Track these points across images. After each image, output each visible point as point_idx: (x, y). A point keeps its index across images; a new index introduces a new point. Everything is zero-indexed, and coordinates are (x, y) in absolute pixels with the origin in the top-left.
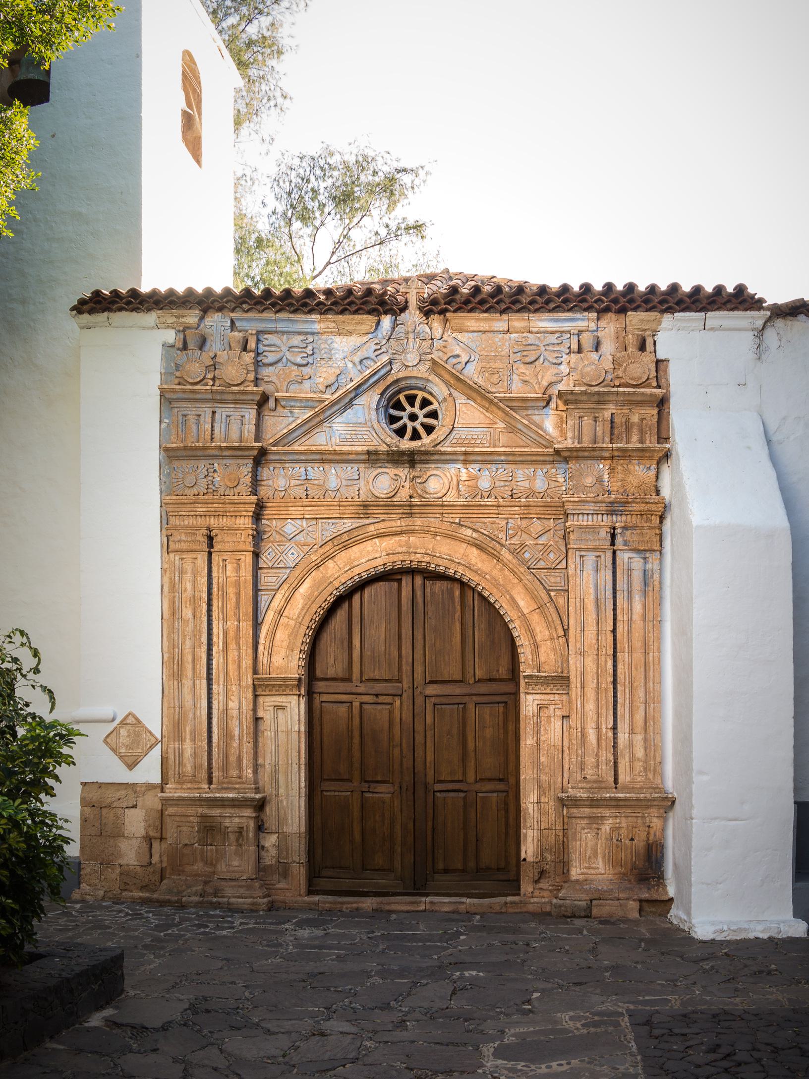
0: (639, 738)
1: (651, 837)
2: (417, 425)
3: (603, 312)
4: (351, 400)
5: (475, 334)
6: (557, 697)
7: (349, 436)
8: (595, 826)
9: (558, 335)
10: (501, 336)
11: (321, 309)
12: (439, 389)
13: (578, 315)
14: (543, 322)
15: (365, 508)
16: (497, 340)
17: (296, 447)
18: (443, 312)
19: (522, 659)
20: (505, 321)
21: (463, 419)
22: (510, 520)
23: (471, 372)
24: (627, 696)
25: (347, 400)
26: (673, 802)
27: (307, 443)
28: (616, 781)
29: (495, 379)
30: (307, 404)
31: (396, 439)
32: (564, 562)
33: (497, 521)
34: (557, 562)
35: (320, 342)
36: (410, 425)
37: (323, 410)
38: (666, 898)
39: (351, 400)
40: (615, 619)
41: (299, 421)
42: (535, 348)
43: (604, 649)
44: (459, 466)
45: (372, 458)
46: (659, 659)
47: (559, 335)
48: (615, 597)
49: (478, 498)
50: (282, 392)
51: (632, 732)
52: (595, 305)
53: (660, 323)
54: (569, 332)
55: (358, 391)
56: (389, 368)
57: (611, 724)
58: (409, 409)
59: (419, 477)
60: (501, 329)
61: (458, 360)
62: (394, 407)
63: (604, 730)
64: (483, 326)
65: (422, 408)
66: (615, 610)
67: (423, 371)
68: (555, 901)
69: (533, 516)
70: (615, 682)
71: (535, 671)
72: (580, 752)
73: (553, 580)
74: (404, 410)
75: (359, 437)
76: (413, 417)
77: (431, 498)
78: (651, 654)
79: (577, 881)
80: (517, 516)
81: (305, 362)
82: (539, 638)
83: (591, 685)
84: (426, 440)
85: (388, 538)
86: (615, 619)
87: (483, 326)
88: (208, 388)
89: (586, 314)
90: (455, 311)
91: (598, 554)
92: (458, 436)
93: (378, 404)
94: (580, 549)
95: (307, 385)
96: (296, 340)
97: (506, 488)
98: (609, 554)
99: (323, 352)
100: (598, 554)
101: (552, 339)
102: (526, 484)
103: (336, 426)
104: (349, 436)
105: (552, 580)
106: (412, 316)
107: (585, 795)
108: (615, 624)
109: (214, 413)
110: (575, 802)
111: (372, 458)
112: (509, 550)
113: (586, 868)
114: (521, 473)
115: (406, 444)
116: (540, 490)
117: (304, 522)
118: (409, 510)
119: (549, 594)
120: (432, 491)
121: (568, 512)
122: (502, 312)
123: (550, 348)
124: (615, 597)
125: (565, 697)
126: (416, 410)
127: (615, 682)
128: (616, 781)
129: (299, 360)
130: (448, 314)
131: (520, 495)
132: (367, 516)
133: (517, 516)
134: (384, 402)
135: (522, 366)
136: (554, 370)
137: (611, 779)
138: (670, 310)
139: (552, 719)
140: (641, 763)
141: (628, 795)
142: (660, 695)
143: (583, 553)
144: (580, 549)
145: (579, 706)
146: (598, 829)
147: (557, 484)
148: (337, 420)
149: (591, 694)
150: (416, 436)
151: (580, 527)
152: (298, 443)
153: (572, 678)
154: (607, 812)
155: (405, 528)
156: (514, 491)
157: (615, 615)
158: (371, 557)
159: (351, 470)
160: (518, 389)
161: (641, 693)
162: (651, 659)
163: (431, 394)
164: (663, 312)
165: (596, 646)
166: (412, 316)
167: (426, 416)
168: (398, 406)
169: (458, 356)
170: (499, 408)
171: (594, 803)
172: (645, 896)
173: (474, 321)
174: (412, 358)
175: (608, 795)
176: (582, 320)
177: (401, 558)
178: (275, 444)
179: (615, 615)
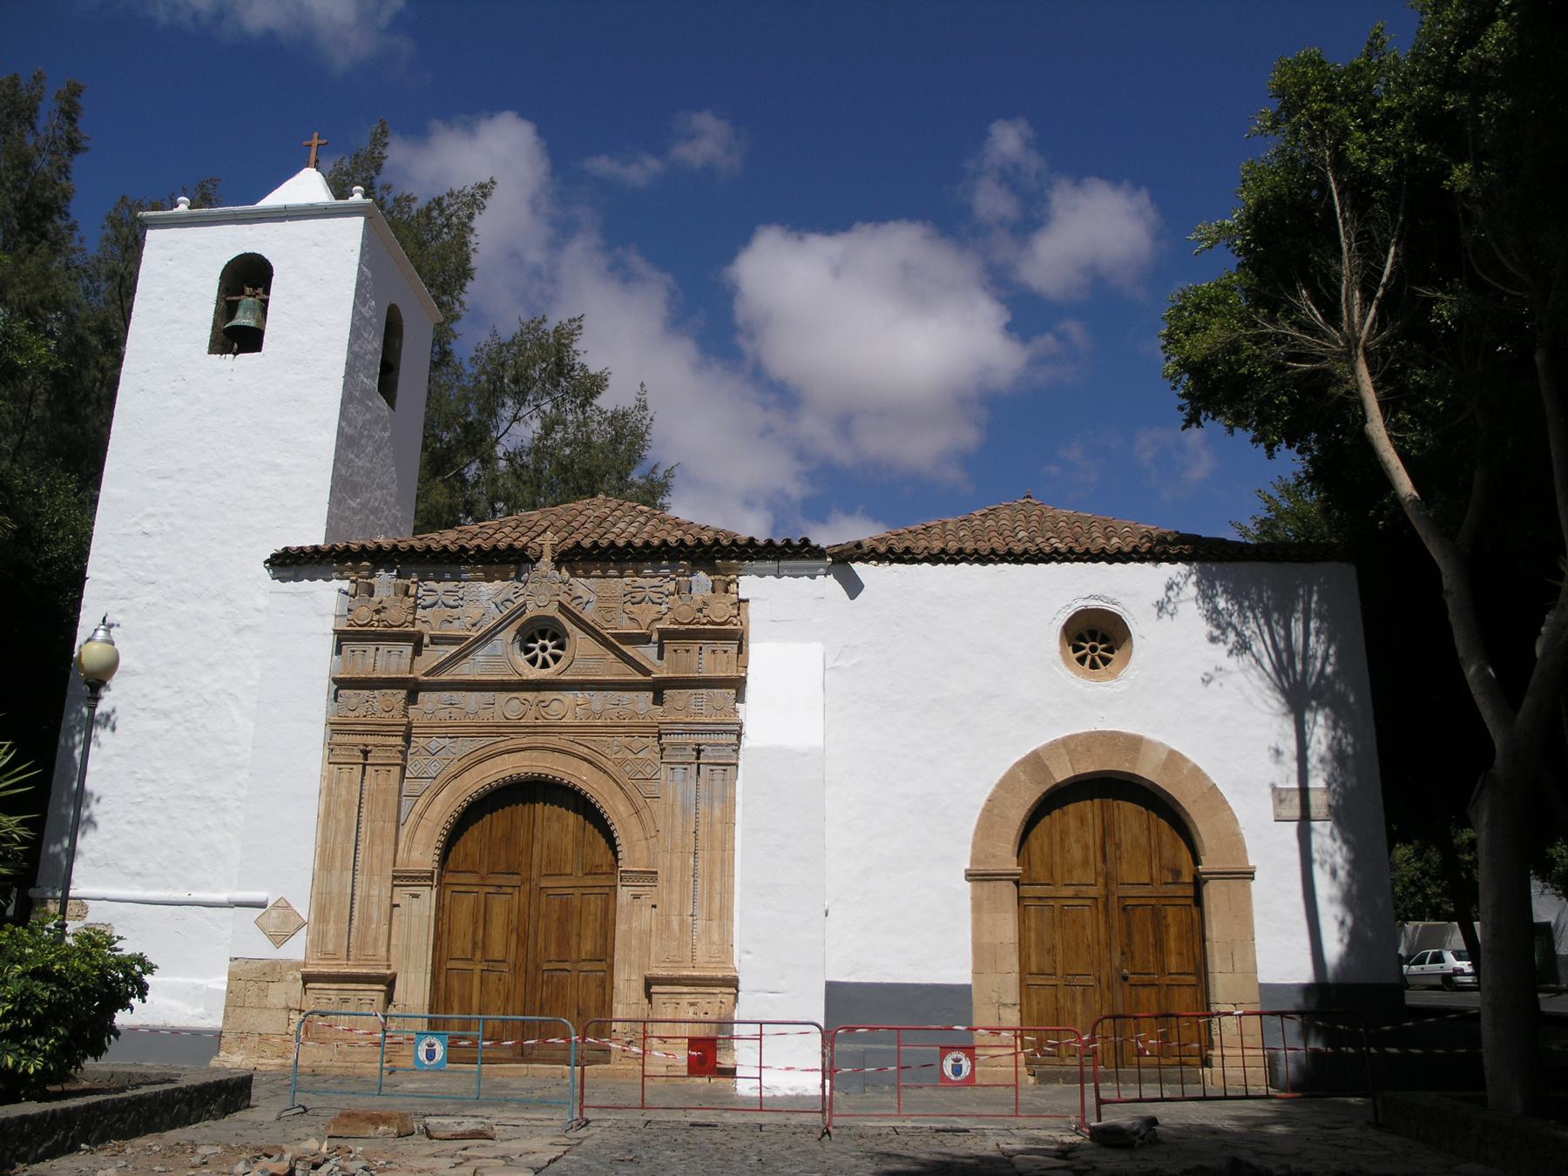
12: (569, 626)
15: (497, 730)
23: (589, 615)
36: (541, 655)
67: (551, 610)
76: (544, 649)
84: (554, 668)
98: (695, 767)
115: (535, 673)
118: (534, 730)
129: (452, 603)
136: (657, 608)
149: (676, 887)
150: (545, 665)
151: (672, 744)
160: (628, 628)
161: (717, 885)
178: (426, 675)
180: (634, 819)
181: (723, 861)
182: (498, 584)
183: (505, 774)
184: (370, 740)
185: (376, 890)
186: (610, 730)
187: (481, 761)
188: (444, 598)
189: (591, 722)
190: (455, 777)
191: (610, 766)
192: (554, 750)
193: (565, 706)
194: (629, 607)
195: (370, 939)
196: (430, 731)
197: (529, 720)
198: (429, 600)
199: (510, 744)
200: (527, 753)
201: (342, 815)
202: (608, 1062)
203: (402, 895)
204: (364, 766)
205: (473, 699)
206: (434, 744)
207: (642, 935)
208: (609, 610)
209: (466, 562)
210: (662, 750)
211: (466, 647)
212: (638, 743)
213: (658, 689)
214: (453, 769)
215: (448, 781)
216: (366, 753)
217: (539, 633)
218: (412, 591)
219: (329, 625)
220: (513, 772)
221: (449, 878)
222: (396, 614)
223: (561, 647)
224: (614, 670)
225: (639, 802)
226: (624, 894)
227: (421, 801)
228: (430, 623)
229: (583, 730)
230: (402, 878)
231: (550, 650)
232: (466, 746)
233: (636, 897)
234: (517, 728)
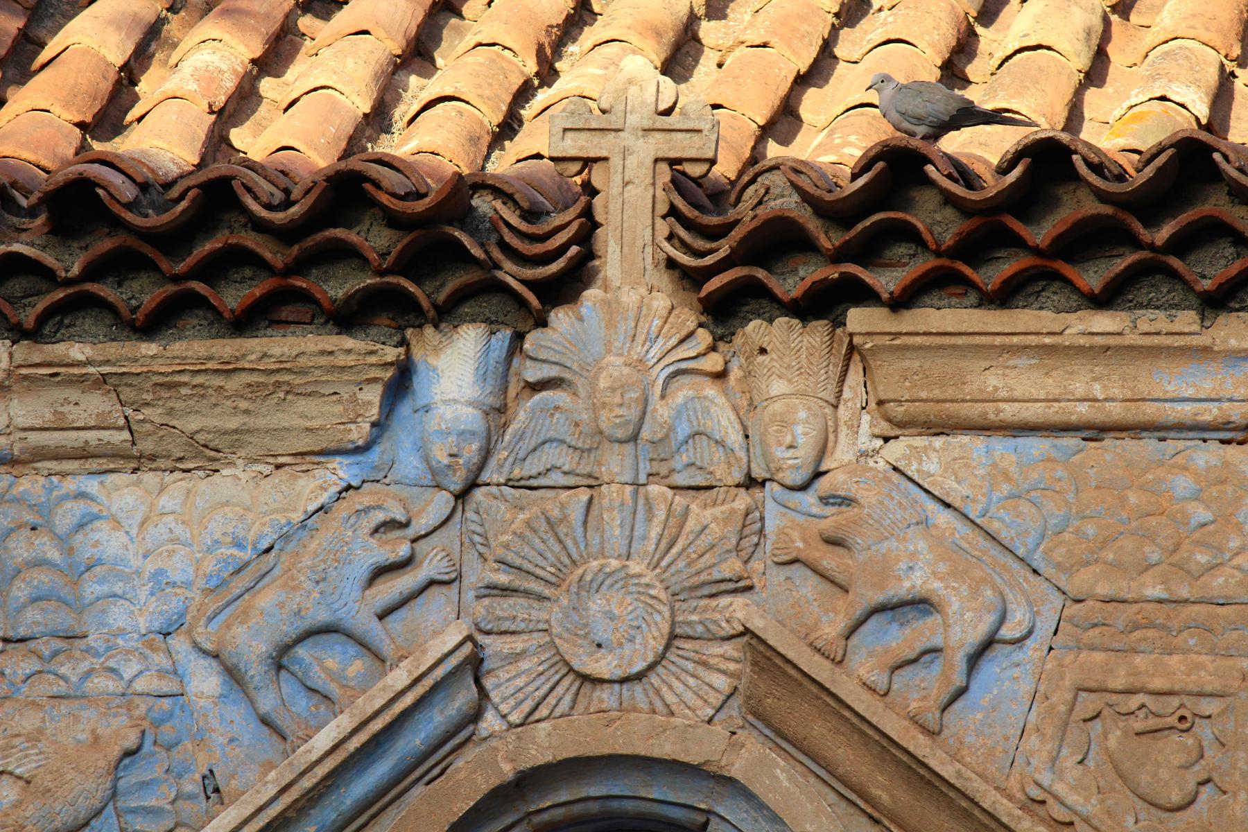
5: (1037, 446)
18: (822, 305)
56: (464, 697)
61: (924, 631)
90: (901, 302)
130: (858, 319)
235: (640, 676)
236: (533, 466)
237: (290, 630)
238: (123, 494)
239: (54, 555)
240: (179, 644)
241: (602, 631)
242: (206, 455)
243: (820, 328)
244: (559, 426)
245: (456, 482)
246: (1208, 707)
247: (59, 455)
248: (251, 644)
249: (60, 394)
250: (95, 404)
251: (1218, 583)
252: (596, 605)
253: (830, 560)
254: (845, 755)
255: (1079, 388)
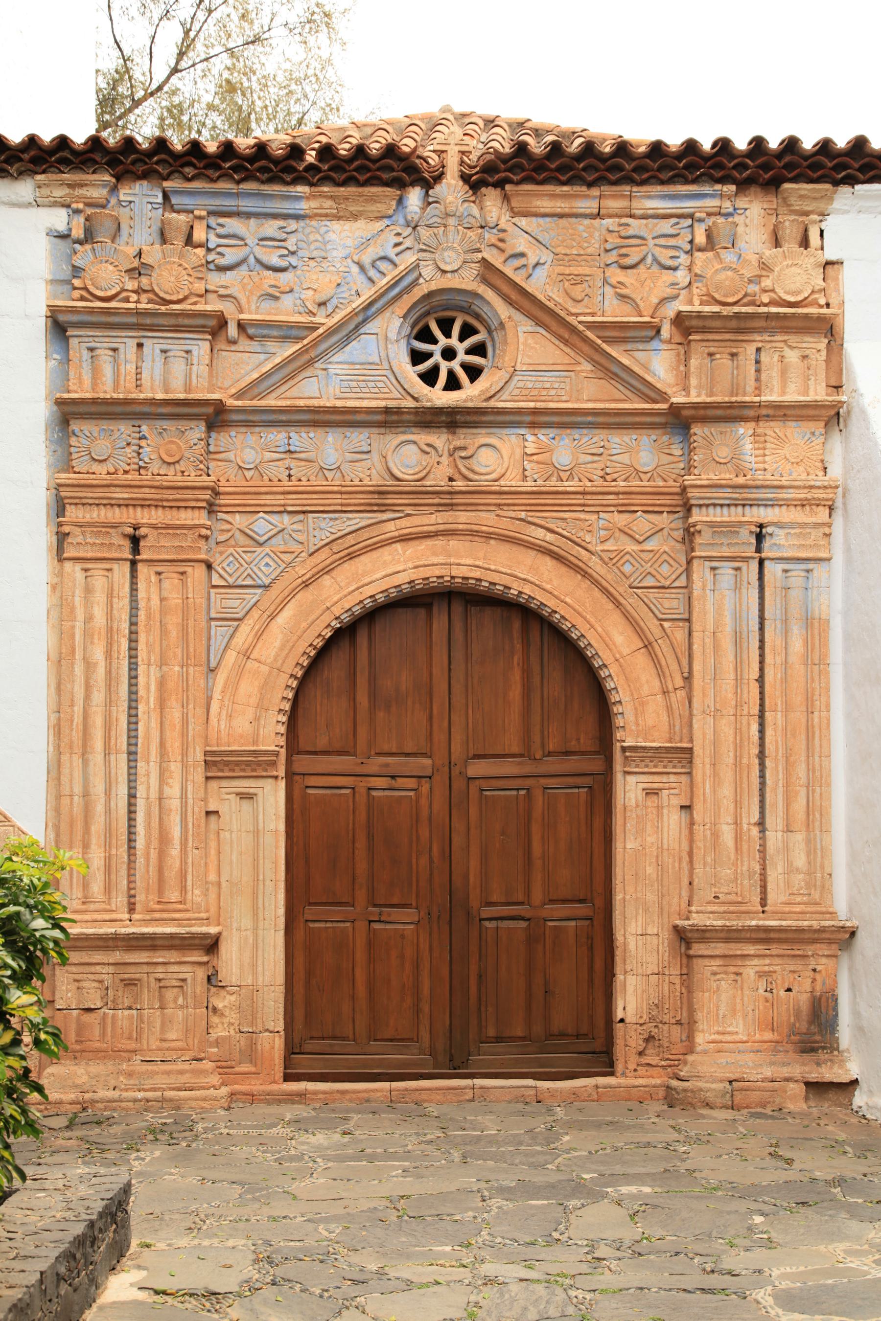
0: (799, 838)
1: (818, 987)
2: (455, 365)
3: (743, 185)
4: (357, 327)
5: (548, 219)
6: (672, 778)
7: (354, 384)
8: (732, 969)
9: (674, 220)
10: (587, 222)
11: (312, 176)
13: (707, 189)
14: (652, 200)
16: (581, 228)
17: (271, 401)
18: (500, 184)
19: (619, 721)
20: (594, 197)
21: (529, 357)
22: (602, 515)
23: (538, 284)
24: (781, 776)
25: (352, 326)
26: (853, 934)
27: (288, 394)
28: (763, 902)
29: (578, 292)
30: (287, 332)
31: (424, 389)
32: (684, 577)
33: (582, 516)
34: (674, 577)
35: (308, 230)
37: (316, 343)
38: (845, 1079)
39: (357, 327)
40: (762, 662)
41: (278, 360)
42: (638, 242)
43: (745, 707)
44: (522, 431)
45: (389, 419)
46: (829, 720)
47: (676, 220)
48: (762, 629)
49: (553, 481)
50: (250, 313)
51: (788, 830)
52: (735, 174)
53: (831, 199)
54: (691, 216)
55: (367, 313)
56: (415, 274)
57: (756, 817)
58: (443, 341)
59: (464, 448)
60: (588, 211)
61: (523, 261)
62: (418, 338)
63: (745, 827)
64: (561, 206)
65: (462, 339)
66: (762, 647)
68: (674, 1083)
69: (635, 508)
70: (762, 756)
71: (640, 740)
72: (709, 859)
73: (672, 603)
74: (435, 341)
75: (371, 384)
76: (449, 354)
77: (483, 482)
78: (816, 714)
79: (705, 1052)
80: (612, 509)
81: (283, 263)
82: (645, 690)
83: (728, 758)
85: (416, 542)
86: (762, 662)
87: (561, 206)
88: (132, 306)
89: (718, 187)
90: (518, 183)
91: (737, 564)
92: (521, 384)
93: (399, 333)
94: (709, 559)
95: (287, 301)
96: (271, 228)
97: (595, 466)
98: (755, 565)
99: (312, 247)
100: (737, 564)
101: (666, 226)
102: (625, 459)
103: (333, 369)
104: (354, 384)
105: (667, 604)
106: (451, 189)
107: (719, 923)
108: (762, 670)
109: (140, 346)
110: (704, 934)
111: (389, 419)
112: (601, 559)
113: (718, 1033)
114: (617, 441)
115: (438, 397)
116: (645, 469)
117: (286, 518)
118: (447, 499)
119: (661, 625)
120: (482, 470)
121: (693, 502)
122: (590, 185)
123: (662, 241)
124: (762, 629)
125: (684, 779)
126: (454, 341)
127: (762, 756)
128: (763, 902)
130: (508, 187)
131: (615, 476)
132: (383, 508)
133: (612, 509)
134: (407, 330)
135: (618, 271)
136: (668, 277)
137: (757, 899)
138: (851, 181)
139: (665, 811)
140: (801, 876)
141: (784, 923)
142: (829, 775)
143: (714, 564)
144: (709, 559)
145: (708, 791)
146: (737, 974)
147: (671, 458)
148: (335, 359)
149: (727, 774)
150: (453, 384)
151: (711, 525)
152: (274, 395)
153: (697, 750)
154: (751, 949)
155: (442, 527)
156: (608, 470)
157: (762, 656)
158: (390, 571)
159: (359, 438)
160: (612, 311)
161: (801, 771)
162: (816, 720)
163: (477, 317)
164: (836, 183)
165: (733, 703)
166: (451, 189)
167: (468, 352)
168: (425, 335)
169: (522, 255)
170: (586, 340)
171: (730, 935)
172: (813, 1077)
173: (547, 198)
174: (451, 259)
175: (754, 923)
176: (712, 196)
177: (438, 573)
178: (239, 395)
179: (762, 656)
180: (642, 659)
181: (809, 729)
182: (361, 228)
183: (402, 579)
184: (143, 516)
185: (172, 787)
186: (585, 500)
187: (351, 557)
188: (260, 252)
189: (553, 483)
190: (306, 585)
191: (595, 565)
192: (488, 536)
193: (498, 457)
194: (616, 275)
195: (171, 875)
196: (252, 502)
197: (438, 479)
198: (230, 256)
199: (406, 525)
200: (439, 542)
201: (98, 654)
202: (612, 1074)
203: (223, 796)
204: (134, 563)
205: (331, 447)
206: (262, 525)
207: (659, 856)
208: (579, 280)
209: (298, 180)
210: (689, 535)
211: (311, 343)
212: (642, 523)
213: (680, 421)
214: (303, 570)
215: (293, 594)
216: (135, 541)
217: (445, 326)
218: (199, 234)
219: (36, 301)
220: (417, 575)
221: (303, 763)
222: (173, 276)
223: (479, 350)
224: (588, 391)
225: (652, 625)
226: (629, 789)
227: (245, 629)
228: (241, 295)
229: (541, 499)
230: (220, 765)
231: (461, 357)
232: (324, 528)
233: (651, 793)
234: (419, 495)
235: (456, 271)
236: (431, 221)
237: (376, 257)
238: (336, 226)
239: (320, 239)
240: (349, 260)
241: (448, 260)
242: (355, 217)
243: (499, 189)
244: (437, 212)
245: (413, 225)
246: (587, 278)
247: (321, 215)
248: (366, 260)
249: (321, 200)
250: (329, 203)
251: (589, 251)
252: (446, 254)
253: (500, 244)
254: (506, 288)
255: (558, 205)
